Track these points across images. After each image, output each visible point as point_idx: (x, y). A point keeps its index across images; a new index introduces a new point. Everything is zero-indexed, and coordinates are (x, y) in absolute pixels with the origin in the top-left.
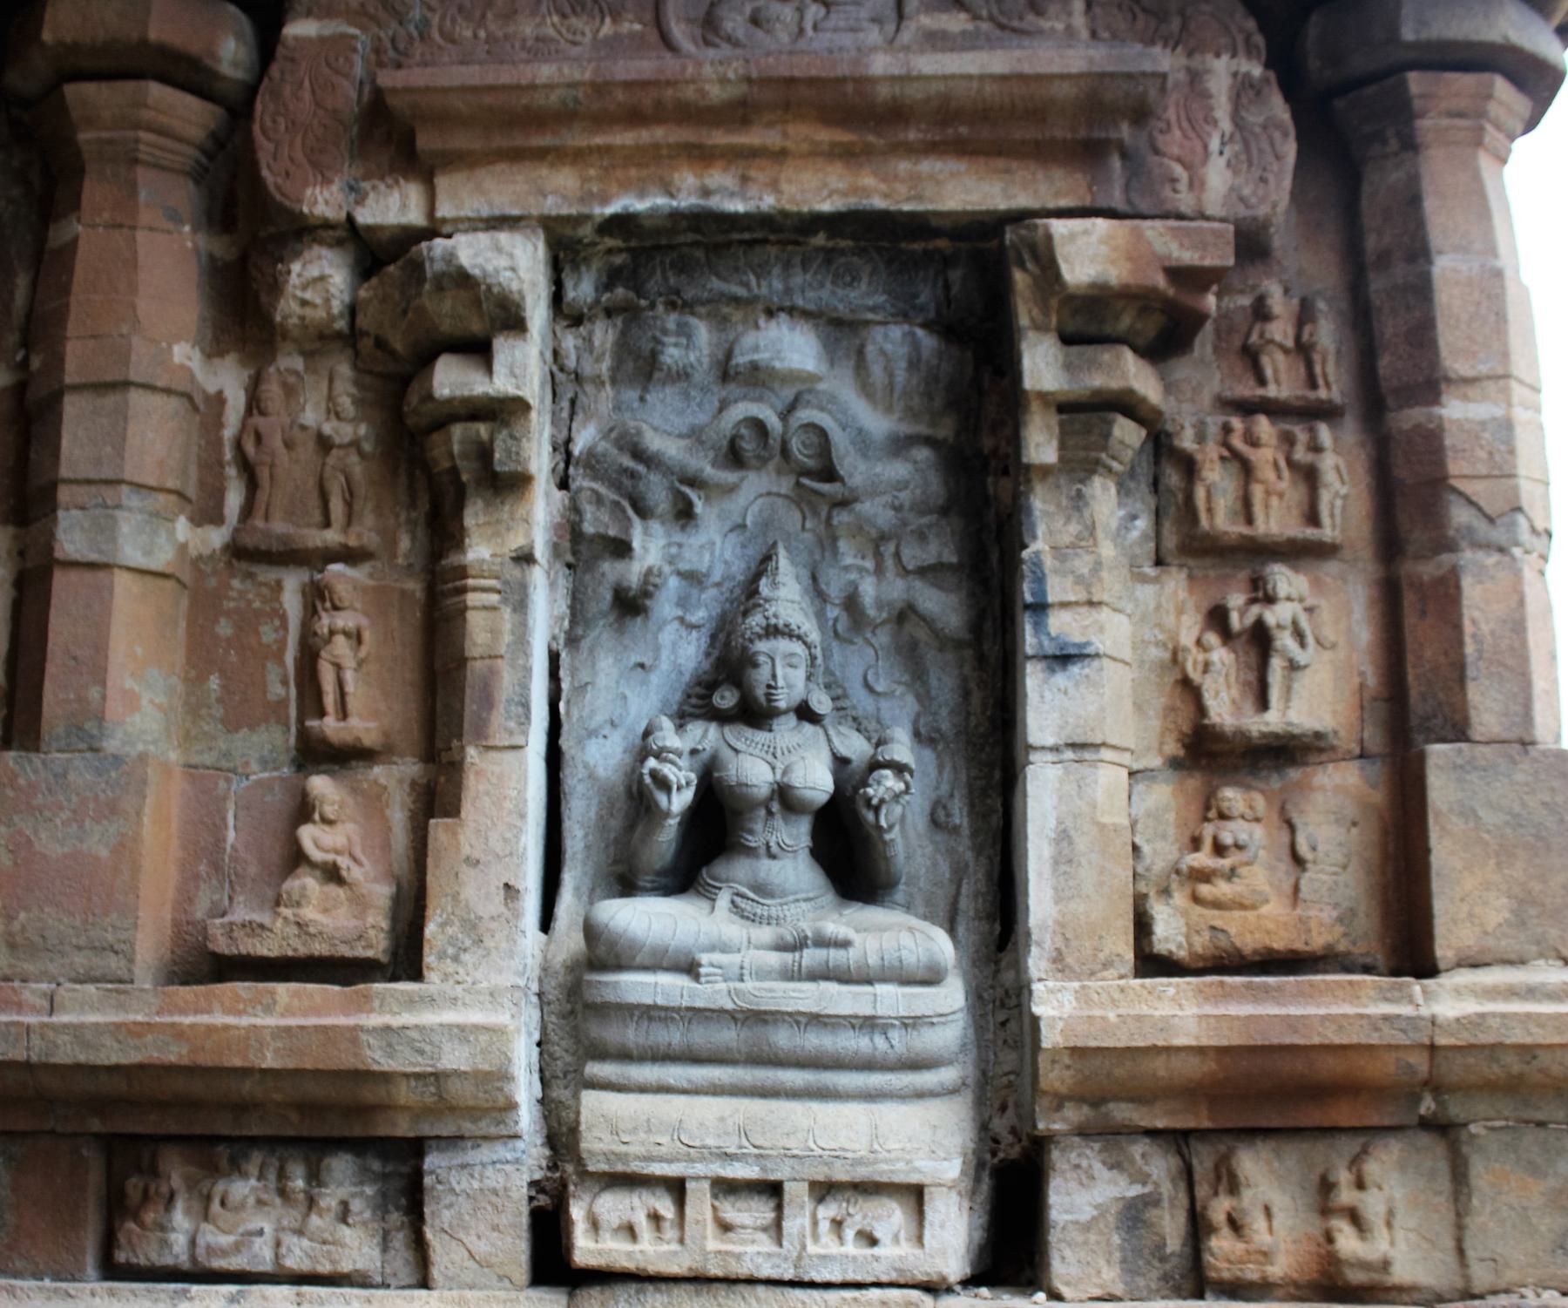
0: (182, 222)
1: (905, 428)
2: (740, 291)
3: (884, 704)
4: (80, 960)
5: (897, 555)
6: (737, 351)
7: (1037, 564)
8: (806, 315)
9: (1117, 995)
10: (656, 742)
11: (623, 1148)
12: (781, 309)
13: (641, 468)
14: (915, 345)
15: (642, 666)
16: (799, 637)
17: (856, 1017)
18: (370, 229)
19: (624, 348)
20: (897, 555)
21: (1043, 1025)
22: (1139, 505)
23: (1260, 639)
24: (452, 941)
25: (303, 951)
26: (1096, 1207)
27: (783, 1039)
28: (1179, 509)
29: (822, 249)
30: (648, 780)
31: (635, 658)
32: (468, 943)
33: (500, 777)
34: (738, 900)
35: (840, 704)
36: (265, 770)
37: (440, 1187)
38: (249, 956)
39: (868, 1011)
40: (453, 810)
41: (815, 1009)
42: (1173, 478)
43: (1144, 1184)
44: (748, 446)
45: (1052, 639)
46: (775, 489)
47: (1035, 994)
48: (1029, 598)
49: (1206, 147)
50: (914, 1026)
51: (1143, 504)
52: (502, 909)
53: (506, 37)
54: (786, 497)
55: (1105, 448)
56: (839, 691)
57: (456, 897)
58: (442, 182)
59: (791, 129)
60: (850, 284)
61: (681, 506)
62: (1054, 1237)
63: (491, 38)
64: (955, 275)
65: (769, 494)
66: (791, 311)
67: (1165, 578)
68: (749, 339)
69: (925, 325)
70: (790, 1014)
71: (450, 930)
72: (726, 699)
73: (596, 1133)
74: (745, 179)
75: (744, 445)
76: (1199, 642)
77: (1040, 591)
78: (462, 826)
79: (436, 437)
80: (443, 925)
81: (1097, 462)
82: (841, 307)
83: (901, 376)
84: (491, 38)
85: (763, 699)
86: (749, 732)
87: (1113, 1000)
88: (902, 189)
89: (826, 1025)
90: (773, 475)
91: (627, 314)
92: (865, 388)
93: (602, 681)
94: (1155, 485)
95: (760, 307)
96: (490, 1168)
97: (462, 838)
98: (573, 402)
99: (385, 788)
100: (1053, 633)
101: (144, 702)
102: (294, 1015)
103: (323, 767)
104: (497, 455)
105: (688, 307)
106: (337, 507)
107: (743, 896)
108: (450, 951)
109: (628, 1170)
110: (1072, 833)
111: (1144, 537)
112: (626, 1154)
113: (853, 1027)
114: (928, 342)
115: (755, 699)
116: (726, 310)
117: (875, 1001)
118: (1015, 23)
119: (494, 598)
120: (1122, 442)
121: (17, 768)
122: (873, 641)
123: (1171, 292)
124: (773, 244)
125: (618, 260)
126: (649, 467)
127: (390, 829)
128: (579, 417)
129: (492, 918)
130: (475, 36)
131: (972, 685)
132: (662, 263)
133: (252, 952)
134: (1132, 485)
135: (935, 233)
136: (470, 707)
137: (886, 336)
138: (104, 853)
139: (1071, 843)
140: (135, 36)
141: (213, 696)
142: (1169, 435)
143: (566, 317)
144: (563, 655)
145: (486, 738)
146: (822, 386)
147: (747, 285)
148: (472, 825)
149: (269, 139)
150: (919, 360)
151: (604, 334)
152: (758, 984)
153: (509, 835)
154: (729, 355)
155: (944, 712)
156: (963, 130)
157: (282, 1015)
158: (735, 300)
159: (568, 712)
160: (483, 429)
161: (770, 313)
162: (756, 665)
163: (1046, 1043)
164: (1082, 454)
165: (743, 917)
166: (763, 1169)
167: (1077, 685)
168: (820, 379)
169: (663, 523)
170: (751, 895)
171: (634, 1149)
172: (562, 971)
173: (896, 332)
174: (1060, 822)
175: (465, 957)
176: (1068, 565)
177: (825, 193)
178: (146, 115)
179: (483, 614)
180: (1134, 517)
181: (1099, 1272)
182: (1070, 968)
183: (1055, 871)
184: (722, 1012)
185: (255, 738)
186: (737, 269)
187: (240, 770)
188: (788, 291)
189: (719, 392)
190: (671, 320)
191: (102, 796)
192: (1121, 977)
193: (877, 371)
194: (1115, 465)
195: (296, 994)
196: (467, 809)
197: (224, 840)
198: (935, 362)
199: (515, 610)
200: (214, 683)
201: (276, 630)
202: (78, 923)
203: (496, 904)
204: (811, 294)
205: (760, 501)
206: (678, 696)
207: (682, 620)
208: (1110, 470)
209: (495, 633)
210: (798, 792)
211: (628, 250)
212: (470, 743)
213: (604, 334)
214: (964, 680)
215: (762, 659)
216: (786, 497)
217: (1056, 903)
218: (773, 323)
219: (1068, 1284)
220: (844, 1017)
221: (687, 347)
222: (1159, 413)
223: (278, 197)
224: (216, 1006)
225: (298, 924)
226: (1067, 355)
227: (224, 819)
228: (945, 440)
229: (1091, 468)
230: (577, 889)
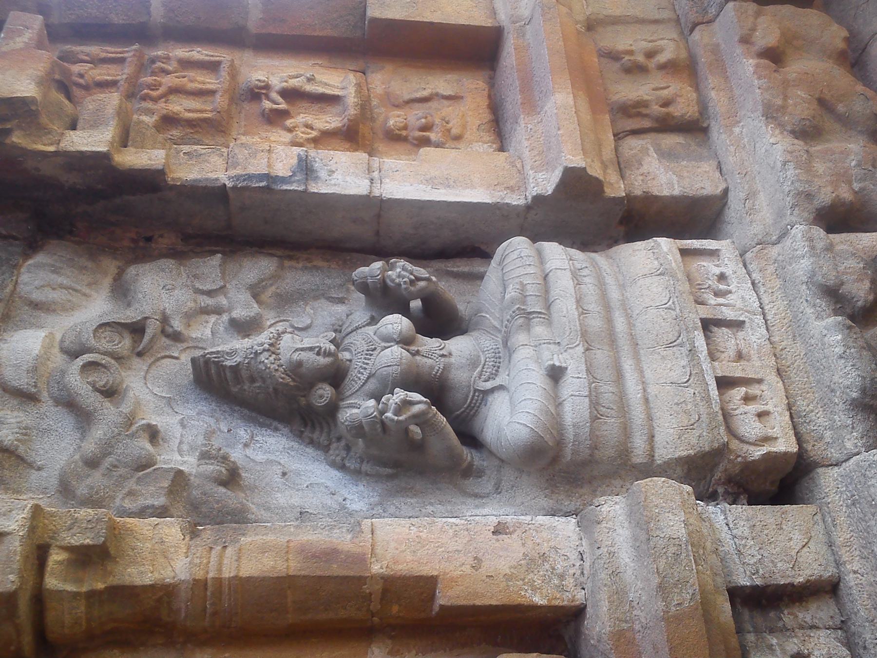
1: (107, 281)
3: (319, 321)
5: (209, 293)
6: (15, 384)
7: (238, 178)
11: (704, 417)
13: (109, 461)
14: (38, 266)
15: (284, 474)
16: (279, 335)
20: (209, 293)
23: (292, 95)
26: (667, 172)
27: (595, 323)
31: (278, 479)
32: (547, 566)
37: (761, 572)
41: (574, 300)
43: (648, 149)
52: (514, 536)
54: (150, 366)
57: (508, 577)
62: (690, 192)
71: (538, 582)
73: (694, 441)
75: (102, 383)
76: (290, 130)
78: (445, 574)
85: (328, 360)
86: (353, 373)
90: (129, 373)
92: (68, 308)
96: (735, 532)
104: (88, 541)
109: (720, 412)
110: (428, 177)
112: (708, 414)
114: (40, 258)
115: (326, 366)
126: (110, 454)
129: (523, 544)
131: (309, 265)
136: (336, 570)
137: (25, 284)
150: (53, 266)
155: (328, 281)
160: (56, 557)
162: (300, 364)
165: (496, 375)
166: (696, 329)
170: (479, 369)
171: (703, 410)
172: (554, 497)
173: (25, 277)
175: (559, 568)
179: (244, 561)
181: (705, 172)
196: (427, 570)
198: (55, 257)
206: (310, 450)
207: (246, 445)
209: (264, 549)
210: (404, 330)
212: (368, 569)
214: (306, 268)
215: (296, 357)
219: (717, 187)
228: (119, 267)
230: (477, 507)
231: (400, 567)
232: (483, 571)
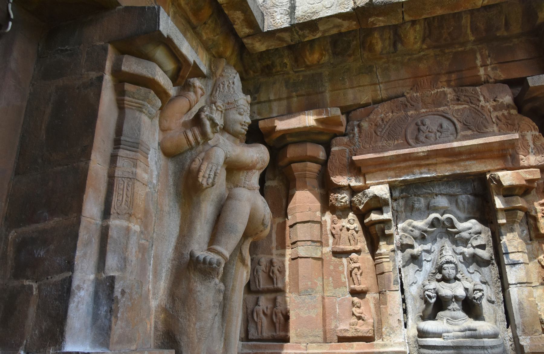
0: (315, 188)
2: (430, 191)
4: (311, 339)
6: (430, 204)
7: (505, 244)
8: (444, 195)
9: (539, 339)
10: (426, 287)
12: (439, 194)
14: (469, 198)
17: (480, 346)
18: (353, 186)
19: (406, 205)
21: (524, 347)
22: (524, 228)
24: (388, 332)
25: (356, 335)
28: (534, 228)
29: (446, 181)
30: (426, 296)
33: (394, 297)
34: (448, 320)
35: (463, 275)
36: (343, 296)
38: (345, 336)
39: (483, 345)
40: (385, 303)
41: (471, 345)
42: (531, 221)
44: (436, 223)
45: (511, 260)
46: (442, 231)
47: (520, 339)
48: (504, 252)
49: (528, 151)
50: (493, 348)
51: (525, 227)
52: (398, 325)
53: (376, 146)
54: (444, 232)
55: (516, 218)
56: (462, 273)
58: (367, 176)
59: (438, 159)
60: (453, 188)
61: (423, 236)
63: (373, 147)
64: (476, 184)
65: (441, 232)
66: (441, 194)
67: (533, 243)
68: (433, 201)
69: (470, 194)
70: (465, 346)
71: (387, 330)
72: (439, 276)
74: (429, 170)
77: (507, 250)
79: (372, 227)
80: (386, 329)
81: (515, 221)
82: (451, 192)
83: (466, 205)
84: (373, 147)
87: (539, 340)
88: (462, 168)
89: (473, 348)
90: (441, 228)
91: (406, 198)
93: (411, 274)
94: (527, 223)
95: (434, 194)
97: (388, 310)
98: (397, 216)
99: (368, 299)
100: (511, 258)
101: (318, 284)
102: (357, 349)
103: (355, 295)
105: (419, 196)
106: (352, 242)
107: (449, 320)
108: (388, 334)
110: (522, 302)
111: (526, 234)
113: (479, 348)
115: (446, 277)
116: (427, 195)
117: (484, 343)
118: (482, 131)
119: (388, 260)
120: (520, 216)
121: (295, 299)
122: (468, 261)
123: (527, 184)
124: (435, 181)
125: (403, 187)
127: (370, 308)
128: (398, 219)
130: (370, 147)
132: (412, 187)
133: (346, 336)
134: (522, 224)
135: (471, 175)
138: (314, 316)
139: (522, 305)
140: (305, 155)
141: (331, 282)
142: (529, 212)
143: (393, 199)
144: (402, 269)
145: (390, 289)
146: (449, 209)
147: (431, 190)
148: (389, 307)
149: (331, 171)
150: (470, 201)
151: (402, 202)
152: (457, 340)
153: (397, 309)
154: (429, 204)
156: (474, 155)
157: (356, 350)
158: (429, 193)
159: (404, 281)
160: (382, 225)
161: (436, 195)
163: (526, 351)
164: (511, 220)
165: (450, 324)
167: (518, 270)
168: (448, 207)
169: (419, 240)
173: (464, 196)
174: (519, 300)
176: (512, 244)
177: (446, 171)
178: (307, 168)
180: (524, 231)
182: (527, 333)
183: (519, 311)
184: (450, 346)
185: (340, 290)
186: (428, 187)
187: (338, 297)
188: (440, 190)
189: (427, 212)
190: (416, 198)
191: (313, 304)
192: (539, 335)
193: (461, 204)
194: (519, 221)
195: (358, 345)
197: (336, 311)
199: (393, 262)
200: (331, 279)
201: (342, 268)
202: (310, 331)
203: (396, 324)
204: (444, 191)
205: (439, 234)
208: (518, 222)
211: (405, 185)
213: (402, 202)
216: (444, 232)
217: (521, 318)
218: (437, 197)
220: (477, 346)
221: (420, 204)
222: (526, 209)
223: (335, 182)
224: (341, 348)
225: (355, 330)
226: (505, 200)
227: (336, 307)
229: (514, 222)
230: (412, 319)
231: (388, 297)
232: (389, 316)
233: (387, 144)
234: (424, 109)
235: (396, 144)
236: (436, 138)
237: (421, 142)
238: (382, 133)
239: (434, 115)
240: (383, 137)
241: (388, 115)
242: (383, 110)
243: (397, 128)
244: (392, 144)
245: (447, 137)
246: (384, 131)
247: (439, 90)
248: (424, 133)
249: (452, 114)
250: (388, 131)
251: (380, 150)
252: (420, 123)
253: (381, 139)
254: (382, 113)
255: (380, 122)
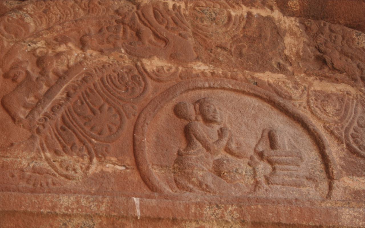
233: (57, 164)
234: (205, 63)
235: (94, 174)
236: (257, 183)
237: (200, 185)
238: (38, 117)
239: (243, 92)
240: (38, 131)
241: (62, 48)
242: (44, 26)
243: (100, 109)
244: (79, 171)
245: (298, 186)
246: (47, 108)
247: (255, 12)
248: (208, 149)
249: (305, 104)
250: (63, 110)
251: (23, 184)
252: (191, 110)
253: (33, 137)
254: (37, 35)
255: (29, 69)
